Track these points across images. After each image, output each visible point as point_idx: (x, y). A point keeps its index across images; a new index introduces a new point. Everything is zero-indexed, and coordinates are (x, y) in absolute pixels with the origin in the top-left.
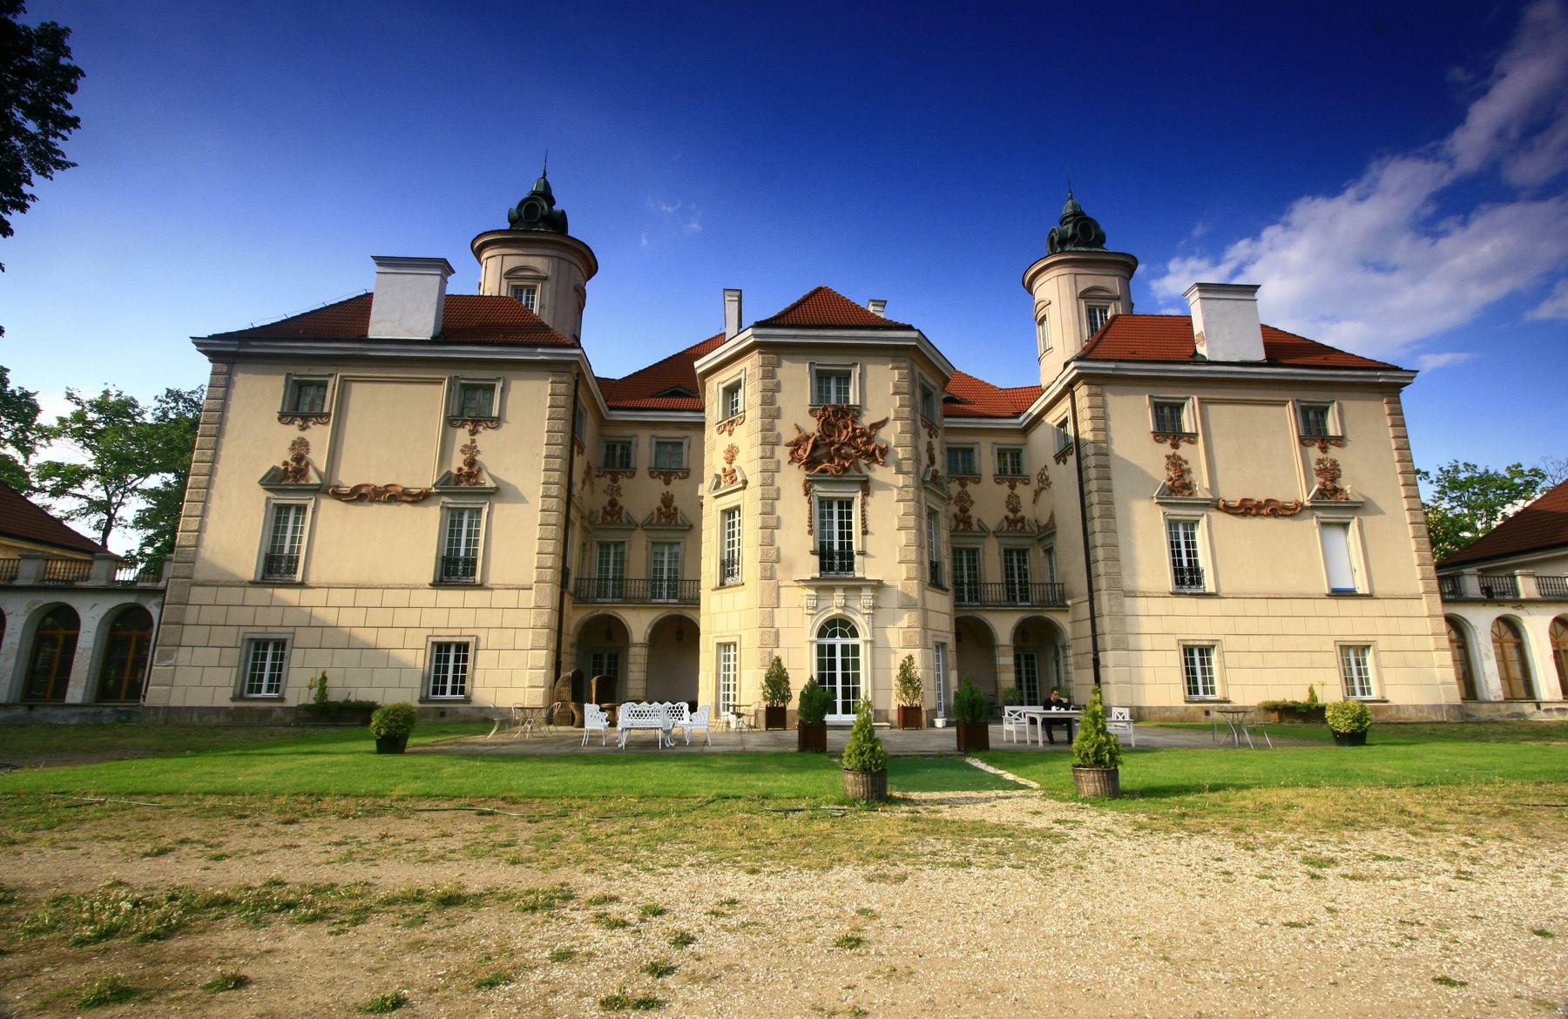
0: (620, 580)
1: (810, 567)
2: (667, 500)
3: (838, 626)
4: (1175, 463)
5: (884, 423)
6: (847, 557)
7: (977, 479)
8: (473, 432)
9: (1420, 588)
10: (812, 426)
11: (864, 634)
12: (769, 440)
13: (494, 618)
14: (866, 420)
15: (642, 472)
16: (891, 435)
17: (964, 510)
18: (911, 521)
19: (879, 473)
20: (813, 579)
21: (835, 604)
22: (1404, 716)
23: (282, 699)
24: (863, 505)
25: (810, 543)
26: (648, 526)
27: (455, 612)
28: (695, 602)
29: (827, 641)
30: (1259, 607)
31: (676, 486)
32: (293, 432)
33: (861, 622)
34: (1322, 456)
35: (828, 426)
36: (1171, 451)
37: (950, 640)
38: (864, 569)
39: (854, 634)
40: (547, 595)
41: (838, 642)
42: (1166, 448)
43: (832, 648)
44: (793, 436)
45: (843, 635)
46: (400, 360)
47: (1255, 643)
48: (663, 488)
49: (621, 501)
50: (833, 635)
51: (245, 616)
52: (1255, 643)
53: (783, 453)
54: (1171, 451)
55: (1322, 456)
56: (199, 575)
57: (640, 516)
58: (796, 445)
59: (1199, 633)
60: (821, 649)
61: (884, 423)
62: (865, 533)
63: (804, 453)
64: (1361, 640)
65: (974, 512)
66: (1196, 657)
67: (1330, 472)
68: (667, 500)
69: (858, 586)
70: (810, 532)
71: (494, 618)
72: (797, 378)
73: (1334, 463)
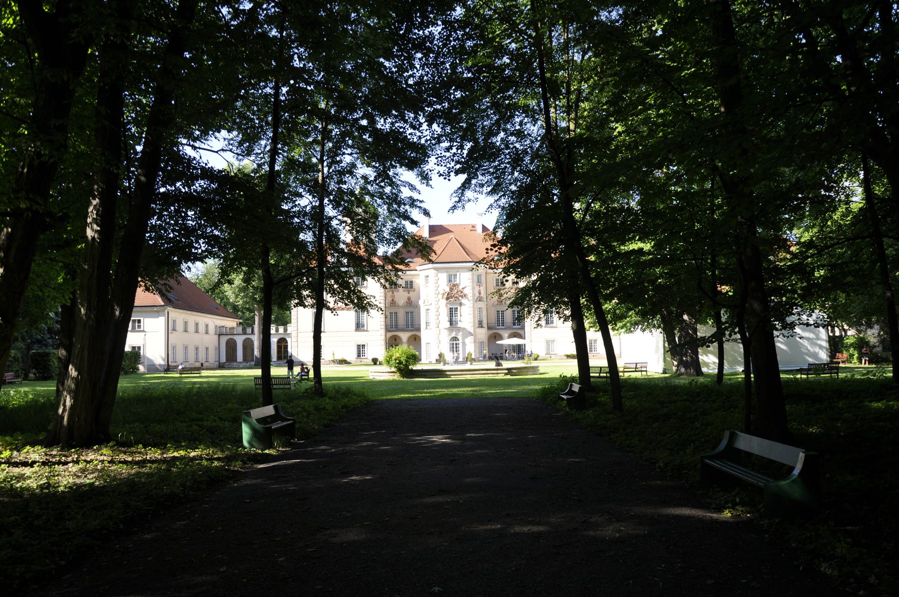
0: (396, 325)
2: (409, 299)
3: (455, 339)
10: (448, 290)
11: (460, 342)
14: (461, 287)
16: (468, 291)
19: (464, 301)
21: (453, 335)
25: (447, 319)
27: (361, 338)
28: (419, 330)
31: (412, 294)
33: (460, 337)
35: (451, 289)
37: (486, 341)
40: (383, 332)
53: (440, 296)
59: (550, 338)
63: (445, 296)
68: (409, 299)
69: (459, 329)
72: (443, 277)
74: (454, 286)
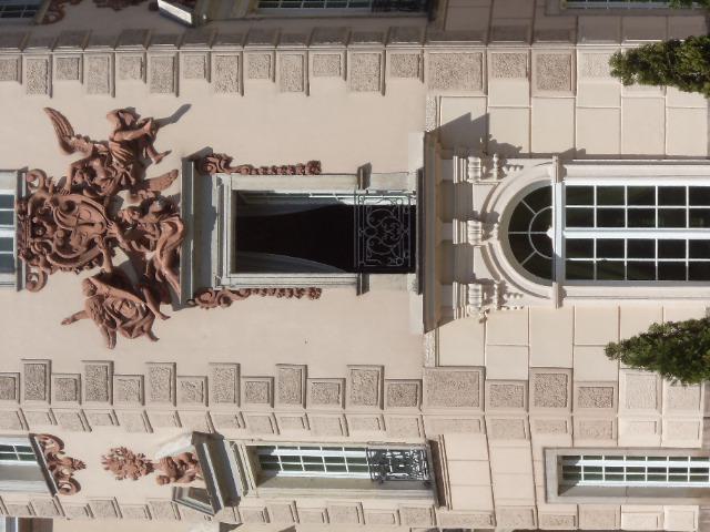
1: (396, 294)
3: (525, 229)
5: (60, 121)
10: (68, 288)
12: (105, 381)
14: (59, 167)
18: (289, 57)
20: (421, 289)
24: (250, 170)
38: (397, 175)
39: (540, 196)
41: (558, 233)
43: (574, 247)
44: (91, 329)
45: (545, 221)
50: (546, 244)
53: (131, 354)
58: (112, 322)
60: (578, 273)
61: (60, 121)
62: (315, 168)
70: (315, 293)
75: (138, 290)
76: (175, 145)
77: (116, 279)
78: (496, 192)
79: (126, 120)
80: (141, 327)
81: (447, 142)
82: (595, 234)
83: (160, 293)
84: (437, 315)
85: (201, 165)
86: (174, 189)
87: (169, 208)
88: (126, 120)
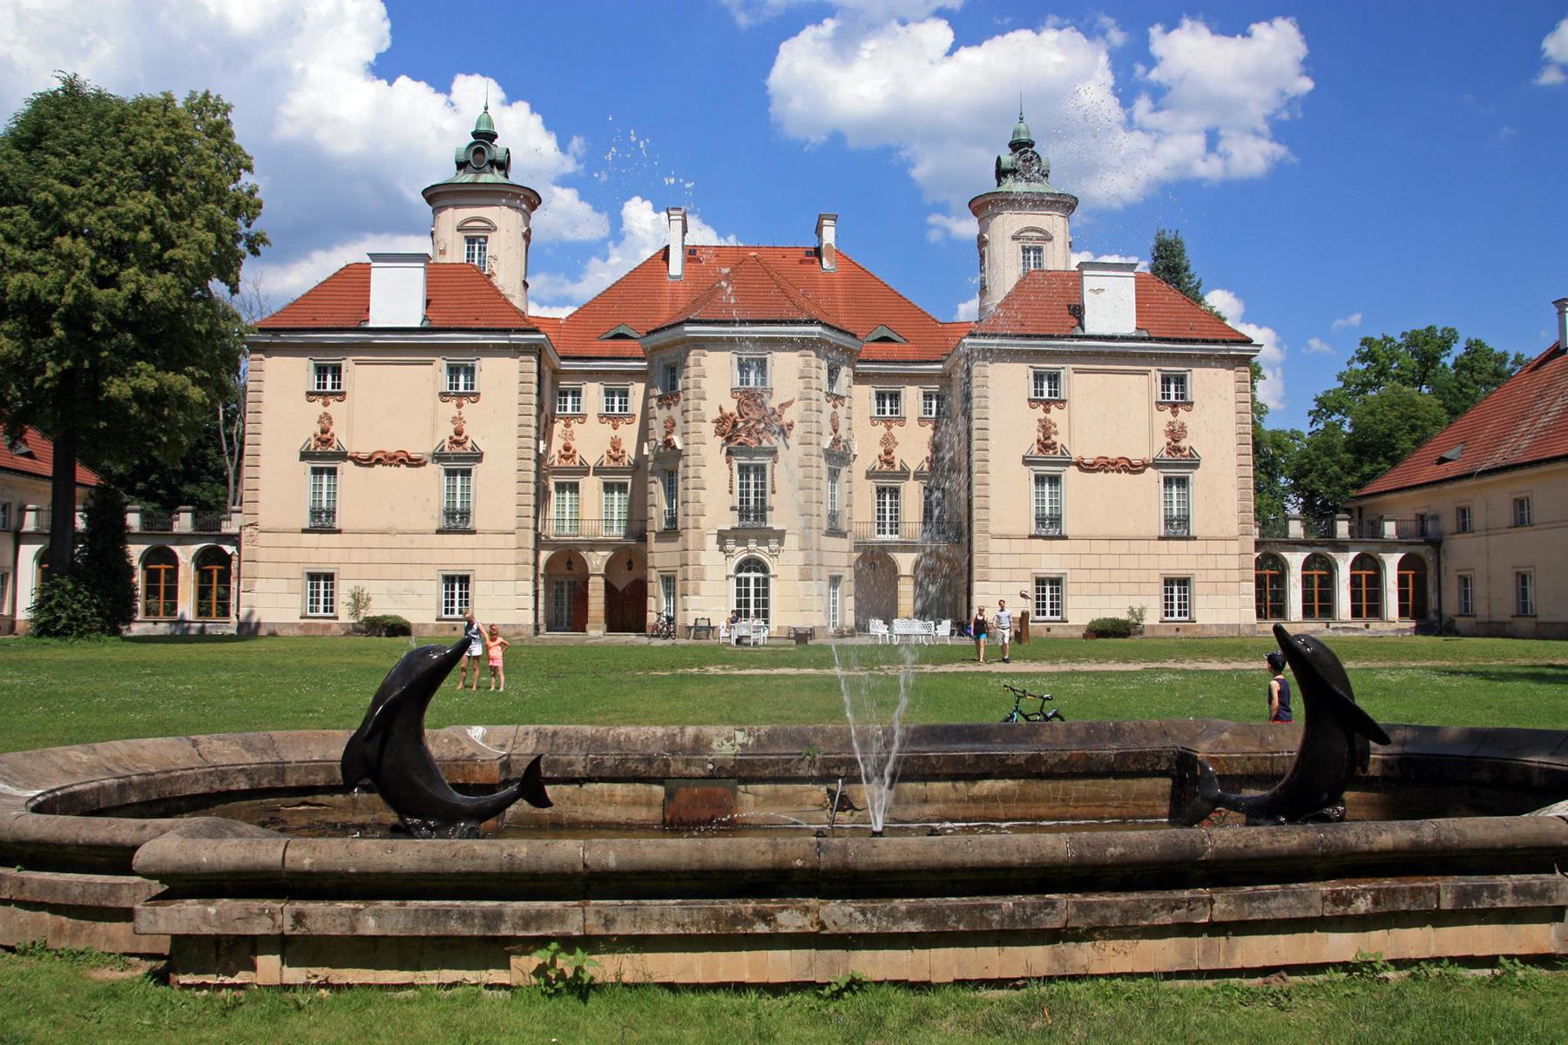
1: (731, 521)
2: (616, 444)
4: (1046, 427)
5: (789, 404)
6: (762, 511)
7: (902, 421)
8: (459, 406)
9: (1234, 529)
10: (731, 407)
13: (488, 556)
14: (773, 403)
15: (592, 419)
17: (888, 453)
20: (733, 529)
22: (1207, 633)
23: (336, 618)
26: (599, 471)
27: (456, 553)
29: (743, 575)
30: (1103, 546)
32: (318, 406)
34: (1172, 419)
36: (1043, 415)
38: (774, 522)
39: (765, 569)
41: (752, 575)
42: (1039, 412)
43: (747, 580)
45: (756, 571)
46: (396, 345)
47: (1095, 576)
48: (613, 433)
49: (574, 445)
50: (748, 571)
51: (301, 555)
52: (1095, 576)
53: (709, 429)
54: (1043, 415)
55: (1172, 419)
56: (262, 525)
57: (592, 462)
60: (739, 581)
61: (789, 404)
64: (1181, 574)
65: (898, 455)
66: (1049, 586)
67: (1176, 434)
68: (616, 444)
71: (488, 556)
73: (1182, 427)
74: (748, 398)
75: (728, 429)
76: (777, 442)
77: (735, 424)
78: (762, 553)
79: (791, 425)
80: (720, 432)
81: (780, 536)
82: (752, 588)
83: (729, 439)
84: (722, 537)
85: (772, 452)
86: (765, 443)
87: (760, 442)
88: (791, 425)
